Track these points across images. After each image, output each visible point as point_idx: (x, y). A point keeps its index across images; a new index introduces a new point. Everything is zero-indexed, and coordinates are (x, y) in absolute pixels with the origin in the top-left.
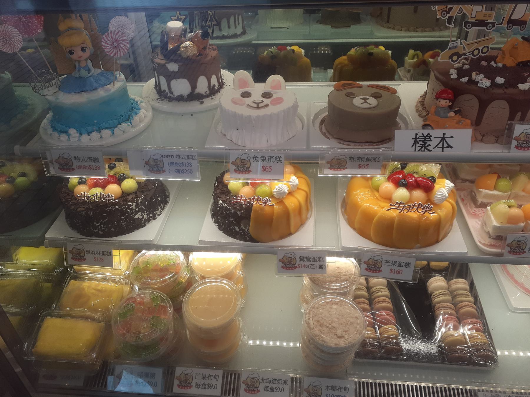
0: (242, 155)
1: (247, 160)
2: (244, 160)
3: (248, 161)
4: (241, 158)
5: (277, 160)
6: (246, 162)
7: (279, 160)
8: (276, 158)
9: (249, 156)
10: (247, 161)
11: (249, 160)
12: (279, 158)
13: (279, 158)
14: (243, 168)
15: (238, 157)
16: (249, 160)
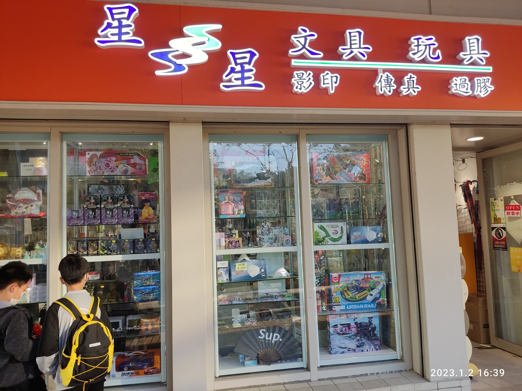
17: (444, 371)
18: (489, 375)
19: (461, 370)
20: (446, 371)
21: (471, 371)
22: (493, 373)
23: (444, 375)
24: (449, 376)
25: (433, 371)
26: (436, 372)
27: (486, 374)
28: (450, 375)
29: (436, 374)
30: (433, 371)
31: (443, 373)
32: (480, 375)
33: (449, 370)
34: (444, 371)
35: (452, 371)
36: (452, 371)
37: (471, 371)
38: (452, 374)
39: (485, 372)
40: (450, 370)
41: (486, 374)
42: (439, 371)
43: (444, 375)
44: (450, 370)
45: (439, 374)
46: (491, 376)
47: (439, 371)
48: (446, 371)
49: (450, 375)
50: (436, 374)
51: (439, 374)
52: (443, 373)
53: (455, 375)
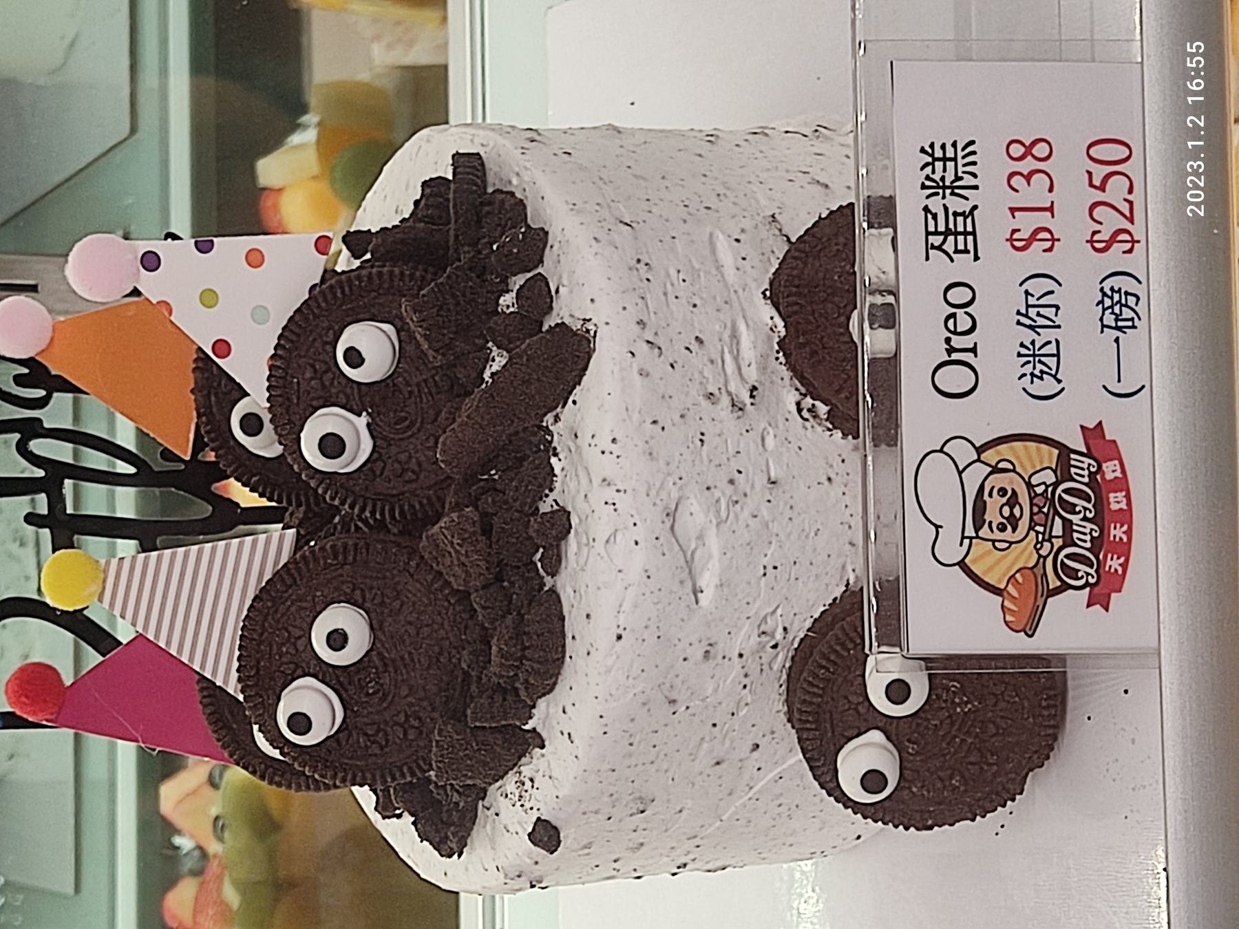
0: (937, 527)
1: (982, 470)
2: (980, 507)
3: (990, 456)
4: (970, 531)
5: (958, 178)
6: (998, 481)
7: (950, 165)
8: (935, 187)
9: (941, 451)
10: (996, 470)
11: (980, 450)
12: (939, 165)
13: (939, 165)
14: (1072, 509)
15: (962, 564)
16: (980, 450)
17: (1191, 186)
18: (1201, 77)
19: (1190, 144)
20: (1191, 181)
21: (1192, 121)
22: (1197, 70)
23: (1202, 184)
24: (1201, 174)
25: (1192, 211)
26: (1193, 204)
27: (1198, 85)
28: (1201, 170)
29: (1198, 205)
30: (1192, 211)
31: (1196, 187)
32: (1202, 99)
33: (1191, 174)
34: (1191, 186)
35: (1192, 167)
36: (1192, 167)
37: (1192, 121)
38: (1199, 166)
39: (1195, 88)
40: (1190, 170)
41: (1198, 85)
42: (1192, 196)
43: (1202, 184)
44: (1190, 170)
45: (1199, 196)
46: (1202, 73)
47: (1192, 196)
48: (1191, 181)
49: (1201, 170)
50: (1198, 205)
51: (1199, 196)
52: (1196, 187)
53: (1201, 159)
